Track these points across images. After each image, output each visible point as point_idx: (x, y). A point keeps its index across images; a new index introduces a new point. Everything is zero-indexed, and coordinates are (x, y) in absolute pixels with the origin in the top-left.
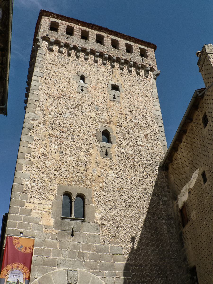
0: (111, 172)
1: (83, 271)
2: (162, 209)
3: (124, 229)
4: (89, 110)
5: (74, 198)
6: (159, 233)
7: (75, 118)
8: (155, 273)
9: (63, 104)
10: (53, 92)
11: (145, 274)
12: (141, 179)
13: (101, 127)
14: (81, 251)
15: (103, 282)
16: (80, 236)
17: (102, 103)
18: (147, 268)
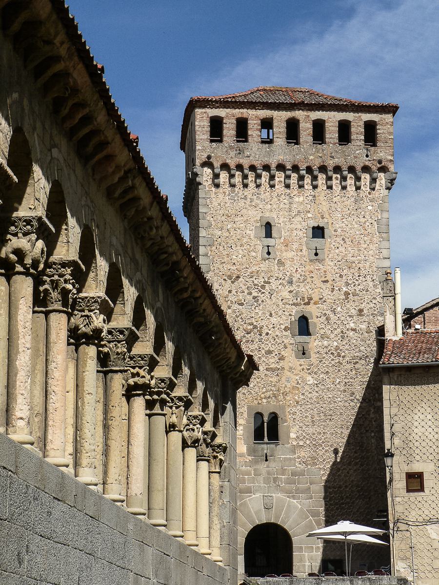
0: (309, 378)
1: (278, 496)
2: (373, 418)
3: (323, 448)
4: (280, 287)
5: (266, 419)
6: (365, 449)
7: (261, 306)
8: (356, 495)
9: (244, 287)
10: (229, 270)
11: (344, 495)
12: (348, 381)
13: (295, 312)
14: (275, 476)
15: (299, 505)
16: (275, 461)
17: (298, 269)
18: (348, 489)
